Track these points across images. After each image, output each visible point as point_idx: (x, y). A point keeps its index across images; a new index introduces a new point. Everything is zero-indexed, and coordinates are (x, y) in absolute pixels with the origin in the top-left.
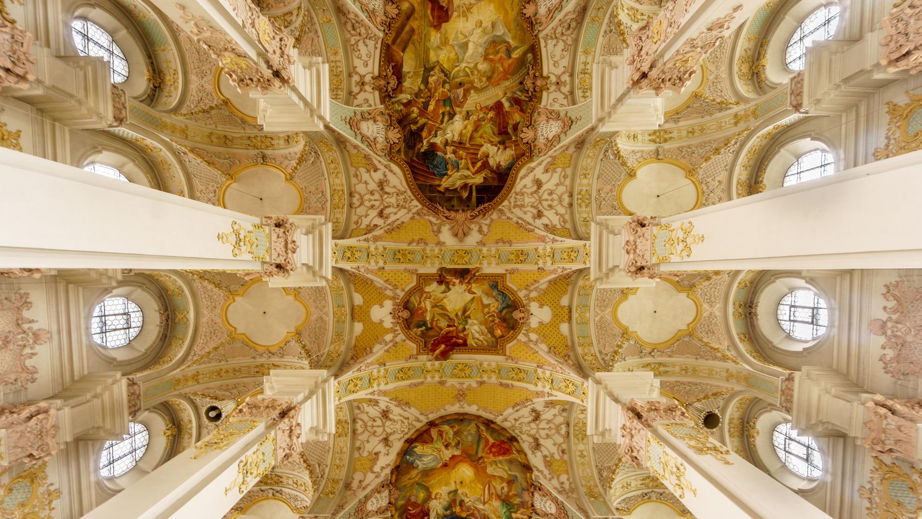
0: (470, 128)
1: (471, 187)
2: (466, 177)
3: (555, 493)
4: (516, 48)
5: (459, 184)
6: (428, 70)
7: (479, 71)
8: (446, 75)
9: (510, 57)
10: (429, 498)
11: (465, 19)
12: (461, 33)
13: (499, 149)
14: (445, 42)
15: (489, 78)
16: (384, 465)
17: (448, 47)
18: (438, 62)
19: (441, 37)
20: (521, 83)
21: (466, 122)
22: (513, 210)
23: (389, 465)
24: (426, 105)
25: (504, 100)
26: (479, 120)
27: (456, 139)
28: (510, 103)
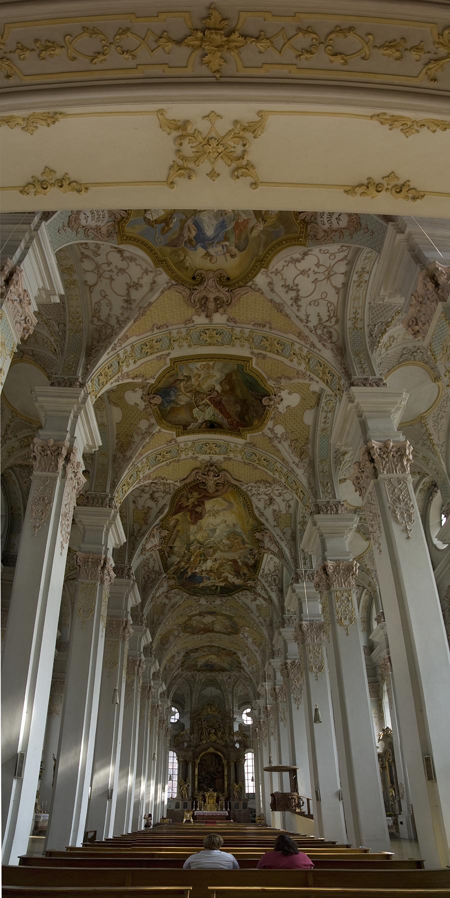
0: (217, 565)
1: (217, 586)
3: (249, 673)
4: (247, 543)
5: (209, 584)
6: (189, 544)
8: (201, 544)
10: (198, 662)
11: (214, 517)
14: (201, 529)
15: (229, 548)
16: (178, 660)
17: (202, 531)
18: (196, 539)
19: (197, 528)
20: (251, 550)
21: (215, 563)
22: (240, 597)
23: (180, 660)
25: (238, 560)
27: (208, 569)
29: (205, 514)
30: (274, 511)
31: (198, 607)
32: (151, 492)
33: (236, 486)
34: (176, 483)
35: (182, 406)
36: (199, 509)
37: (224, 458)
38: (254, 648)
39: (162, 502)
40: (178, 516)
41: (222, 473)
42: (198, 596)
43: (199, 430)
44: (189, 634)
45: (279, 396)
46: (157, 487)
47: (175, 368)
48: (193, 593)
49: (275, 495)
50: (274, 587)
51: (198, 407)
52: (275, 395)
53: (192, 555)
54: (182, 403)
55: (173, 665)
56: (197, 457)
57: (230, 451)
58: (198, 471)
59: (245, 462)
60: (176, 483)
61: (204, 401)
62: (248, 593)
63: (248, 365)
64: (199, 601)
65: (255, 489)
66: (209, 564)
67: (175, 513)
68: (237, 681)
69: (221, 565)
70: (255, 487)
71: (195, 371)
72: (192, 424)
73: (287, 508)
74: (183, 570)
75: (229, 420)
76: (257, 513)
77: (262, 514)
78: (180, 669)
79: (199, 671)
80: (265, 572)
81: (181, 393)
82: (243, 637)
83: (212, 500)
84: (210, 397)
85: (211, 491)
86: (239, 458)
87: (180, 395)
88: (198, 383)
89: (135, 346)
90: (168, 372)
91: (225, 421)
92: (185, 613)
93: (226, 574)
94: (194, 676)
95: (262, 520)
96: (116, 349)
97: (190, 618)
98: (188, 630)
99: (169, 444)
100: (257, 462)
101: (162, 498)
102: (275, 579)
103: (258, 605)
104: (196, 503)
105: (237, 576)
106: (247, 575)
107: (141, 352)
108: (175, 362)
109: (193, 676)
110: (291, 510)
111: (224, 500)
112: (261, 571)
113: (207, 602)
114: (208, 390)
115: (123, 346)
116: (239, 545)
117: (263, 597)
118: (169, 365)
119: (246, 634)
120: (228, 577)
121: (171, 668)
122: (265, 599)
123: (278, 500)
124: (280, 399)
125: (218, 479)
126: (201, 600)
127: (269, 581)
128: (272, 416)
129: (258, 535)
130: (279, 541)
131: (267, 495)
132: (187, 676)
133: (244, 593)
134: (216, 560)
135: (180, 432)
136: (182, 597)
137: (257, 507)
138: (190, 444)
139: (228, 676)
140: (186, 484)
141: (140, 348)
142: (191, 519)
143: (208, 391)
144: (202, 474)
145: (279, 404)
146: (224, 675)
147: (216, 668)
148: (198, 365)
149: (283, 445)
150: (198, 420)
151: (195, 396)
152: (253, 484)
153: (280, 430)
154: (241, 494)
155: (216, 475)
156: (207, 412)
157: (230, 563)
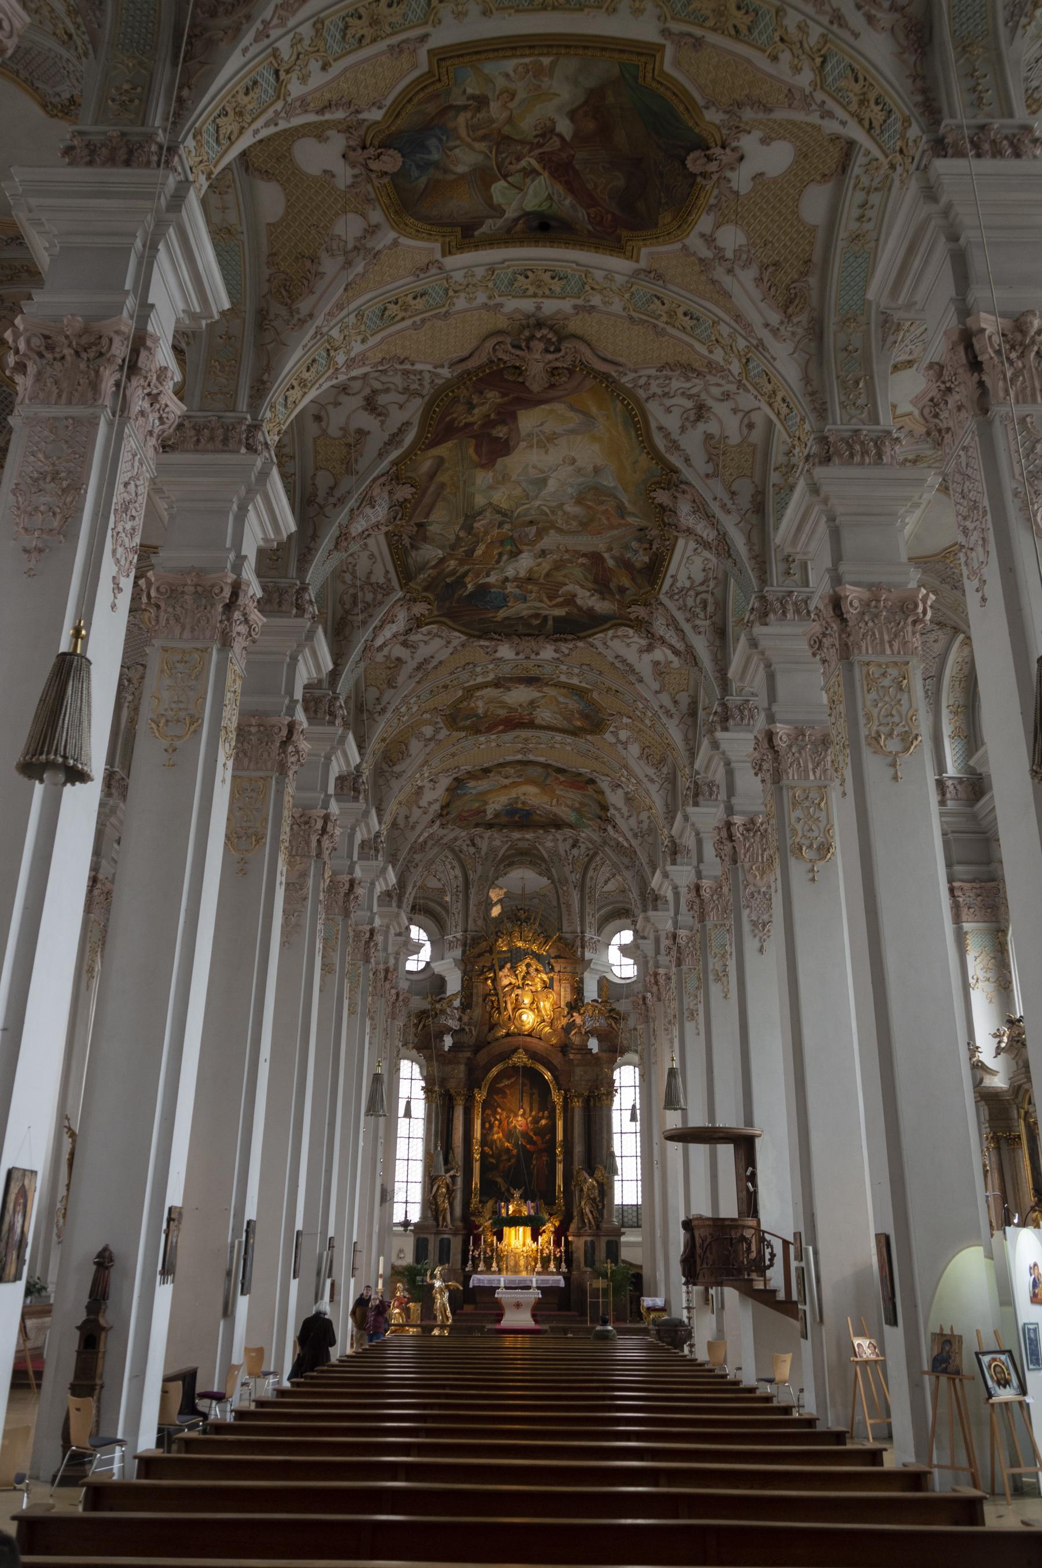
0: (546, 566)
1: (546, 617)
2: (539, 608)
3: (629, 835)
4: (634, 515)
5: (525, 613)
7: (565, 513)
9: (623, 518)
12: (534, 467)
13: (593, 595)
14: (505, 478)
15: (581, 524)
18: (491, 504)
20: (641, 530)
21: (540, 560)
22: (610, 643)
24: (470, 553)
25: (606, 555)
26: (561, 560)
28: (617, 563)
29: (518, 443)
30: (708, 437)
31: (491, 666)
32: (367, 391)
33: (606, 376)
34: (439, 371)
35: (462, 177)
36: (500, 432)
37: (575, 307)
38: (642, 769)
39: (396, 418)
40: (442, 450)
41: (565, 345)
42: (492, 639)
43: (507, 237)
44: (463, 734)
45: (733, 150)
46: (384, 378)
47: (444, 78)
48: (477, 633)
49: (712, 397)
50: (704, 624)
51: (505, 177)
52: (724, 147)
53: (478, 542)
54: (461, 169)
55: (416, 813)
56: (501, 305)
57: (592, 289)
58: (500, 339)
59: (631, 318)
60: (439, 371)
61: (523, 163)
62: (631, 632)
63: (650, 67)
64: (496, 651)
65: (658, 382)
66: (525, 563)
67: (435, 443)
68: (596, 854)
69: (558, 565)
70: (657, 378)
71: (501, 82)
72: (489, 222)
73: (745, 431)
74: (452, 578)
75: (592, 210)
76: (660, 443)
77: (675, 446)
78: (438, 823)
79: (490, 826)
80: (679, 585)
81: (458, 142)
82: (613, 740)
83: (538, 409)
84: (540, 150)
85: (535, 388)
86: (617, 307)
87: (455, 147)
88: (505, 114)
89: (327, 22)
90: (422, 89)
91: (581, 214)
92: (455, 683)
93: (570, 588)
94: (477, 841)
95: (675, 460)
96: (268, 36)
97: (470, 692)
98: (461, 724)
99: (422, 276)
100: (664, 318)
101: (397, 406)
102: (705, 604)
103: (657, 663)
104: (493, 417)
105: (601, 593)
106: (628, 592)
107: (344, 37)
108: (444, 59)
109: (472, 841)
110: (757, 436)
111: (572, 408)
112: (668, 581)
113: (517, 654)
114: (534, 133)
115: (291, 23)
116: (608, 519)
117: (671, 647)
118: (424, 68)
119: (623, 735)
120: (576, 596)
121: (412, 820)
122: (676, 652)
123: (722, 409)
124: (737, 155)
125: (556, 359)
126: (500, 648)
127: (689, 606)
128: (712, 201)
129: (662, 497)
130: (719, 513)
131: (690, 397)
132: (456, 839)
133: (619, 633)
134: (543, 553)
135: (453, 244)
136: (449, 642)
137: (661, 428)
138: (480, 272)
139: (571, 841)
140: (468, 373)
141: (341, 25)
142: (480, 457)
143: (536, 136)
144: (514, 346)
145: (732, 169)
146: (558, 836)
147: (537, 818)
148: (510, 65)
149: (739, 282)
150: (505, 211)
151: (497, 149)
152: (653, 372)
153: (731, 238)
154: (618, 395)
155: (552, 349)
156: (531, 191)
157: (580, 560)
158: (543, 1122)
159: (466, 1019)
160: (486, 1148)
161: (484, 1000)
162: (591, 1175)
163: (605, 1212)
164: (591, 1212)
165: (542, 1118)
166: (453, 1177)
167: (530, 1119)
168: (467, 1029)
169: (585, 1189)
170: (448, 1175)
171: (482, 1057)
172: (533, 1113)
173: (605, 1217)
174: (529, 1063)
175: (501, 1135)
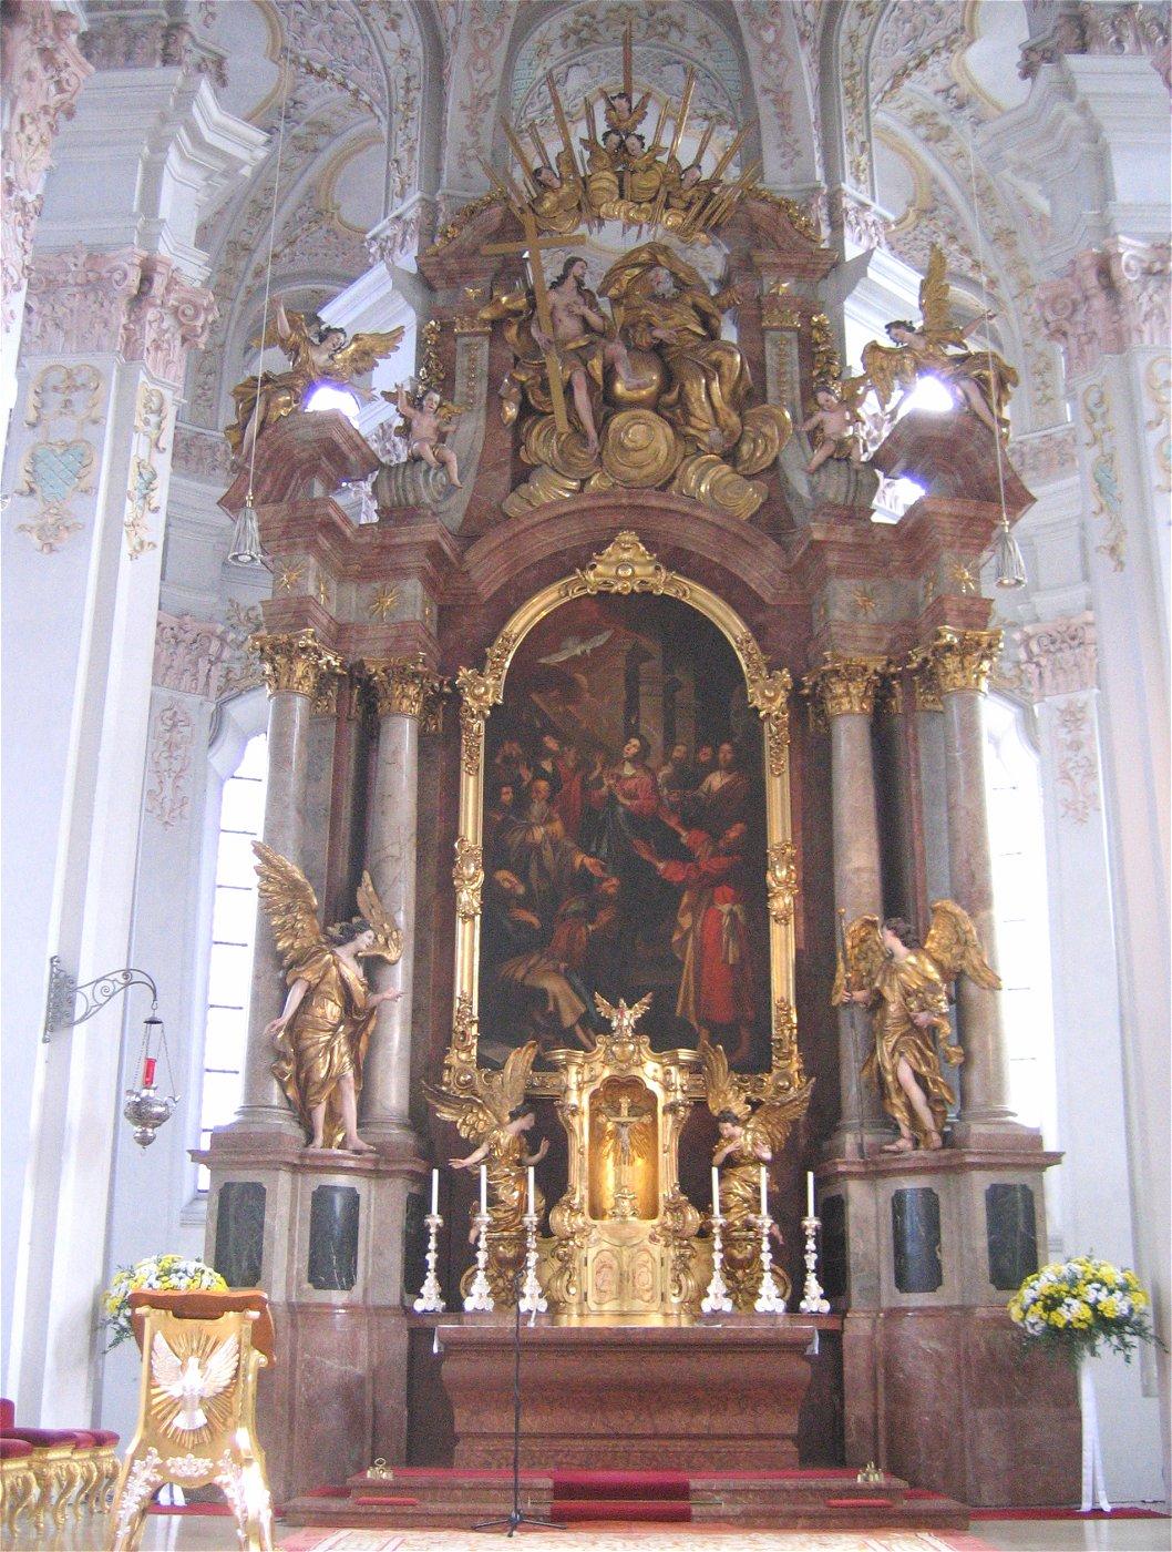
158: (716, 781)
159: (425, 424)
160: (502, 875)
161: (494, 383)
162: (914, 942)
163: (975, 1078)
164: (919, 1079)
165: (713, 766)
166: (373, 966)
167: (666, 771)
168: (429, 455)
169: (893, 997)
170: (344, 953)
171: (486, 571)
172: (679, 751)
173: (977, 1097)
174: (663, 583)
175: (558, 827)
